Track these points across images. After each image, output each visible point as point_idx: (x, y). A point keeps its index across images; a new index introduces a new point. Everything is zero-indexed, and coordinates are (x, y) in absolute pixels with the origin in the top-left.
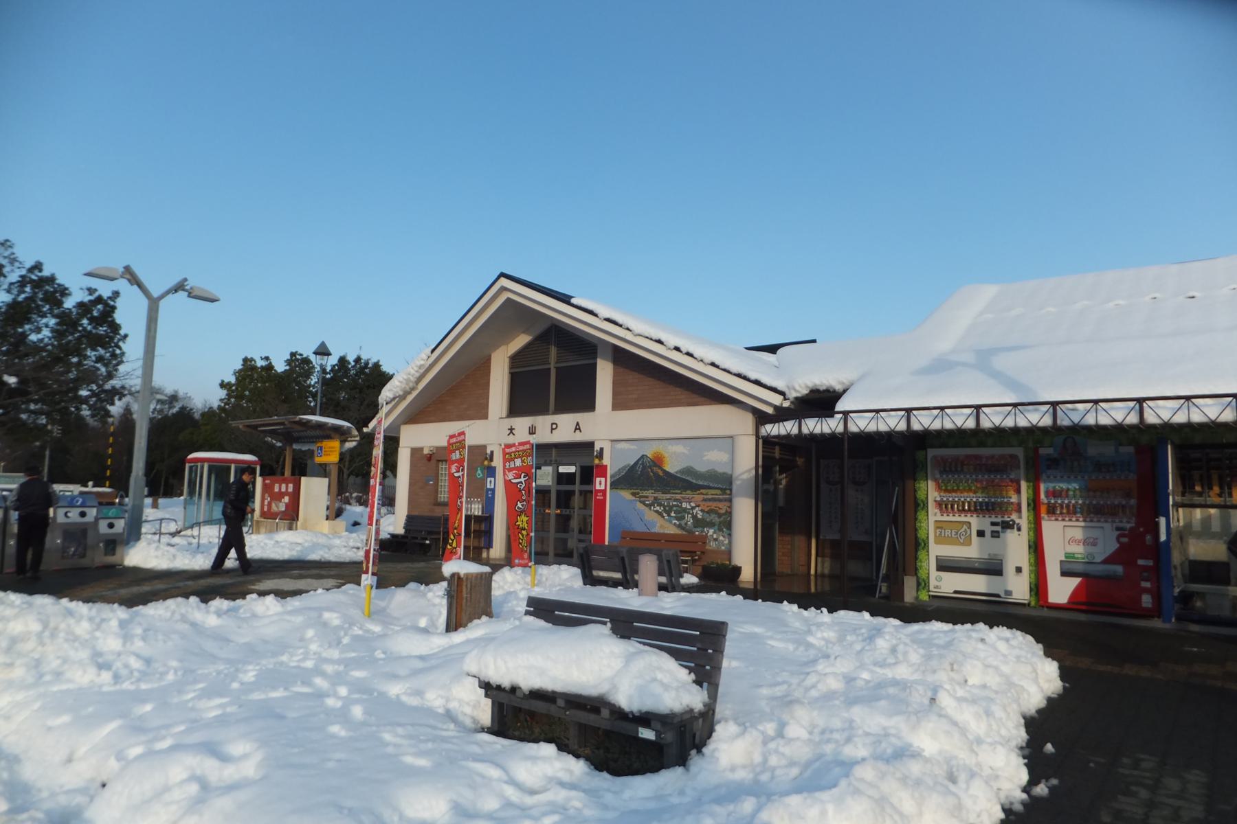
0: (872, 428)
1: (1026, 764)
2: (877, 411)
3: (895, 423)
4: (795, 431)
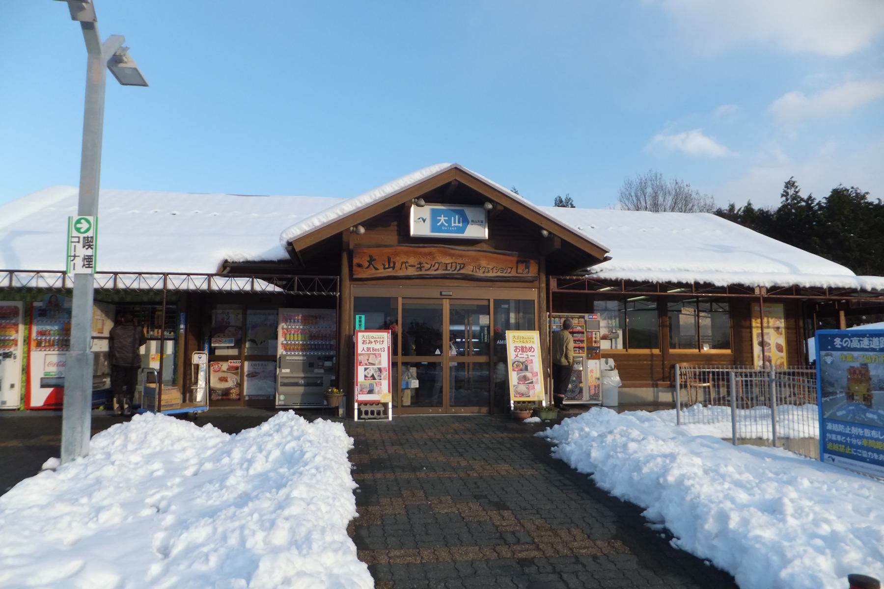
0: (135, 286)
1: (354, 492)
2: (140, 274)
3: (155, 283)
4: (248, 288)
